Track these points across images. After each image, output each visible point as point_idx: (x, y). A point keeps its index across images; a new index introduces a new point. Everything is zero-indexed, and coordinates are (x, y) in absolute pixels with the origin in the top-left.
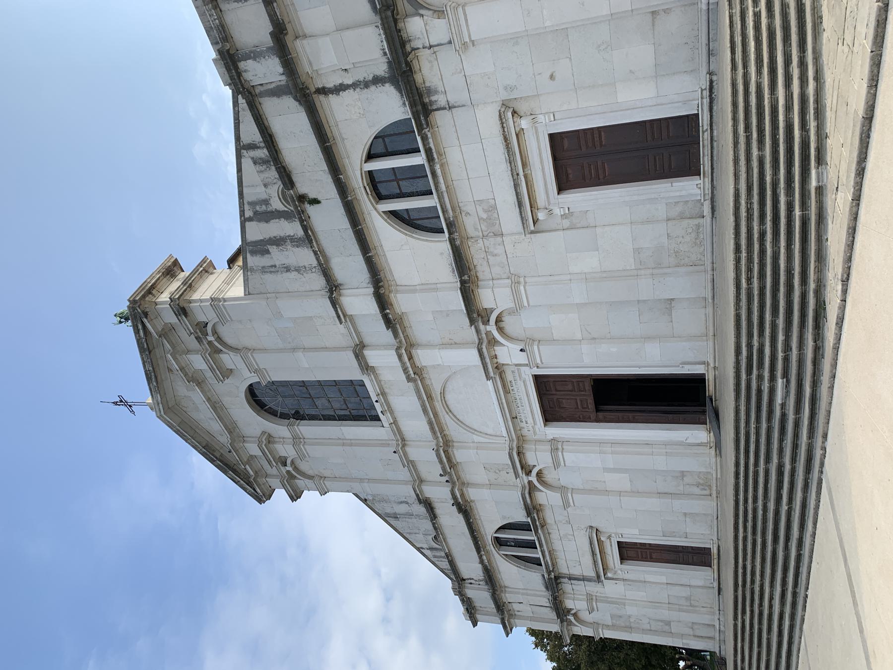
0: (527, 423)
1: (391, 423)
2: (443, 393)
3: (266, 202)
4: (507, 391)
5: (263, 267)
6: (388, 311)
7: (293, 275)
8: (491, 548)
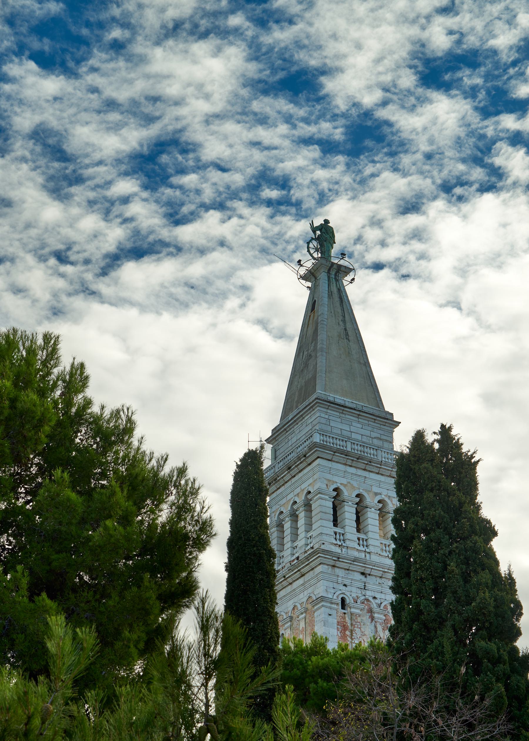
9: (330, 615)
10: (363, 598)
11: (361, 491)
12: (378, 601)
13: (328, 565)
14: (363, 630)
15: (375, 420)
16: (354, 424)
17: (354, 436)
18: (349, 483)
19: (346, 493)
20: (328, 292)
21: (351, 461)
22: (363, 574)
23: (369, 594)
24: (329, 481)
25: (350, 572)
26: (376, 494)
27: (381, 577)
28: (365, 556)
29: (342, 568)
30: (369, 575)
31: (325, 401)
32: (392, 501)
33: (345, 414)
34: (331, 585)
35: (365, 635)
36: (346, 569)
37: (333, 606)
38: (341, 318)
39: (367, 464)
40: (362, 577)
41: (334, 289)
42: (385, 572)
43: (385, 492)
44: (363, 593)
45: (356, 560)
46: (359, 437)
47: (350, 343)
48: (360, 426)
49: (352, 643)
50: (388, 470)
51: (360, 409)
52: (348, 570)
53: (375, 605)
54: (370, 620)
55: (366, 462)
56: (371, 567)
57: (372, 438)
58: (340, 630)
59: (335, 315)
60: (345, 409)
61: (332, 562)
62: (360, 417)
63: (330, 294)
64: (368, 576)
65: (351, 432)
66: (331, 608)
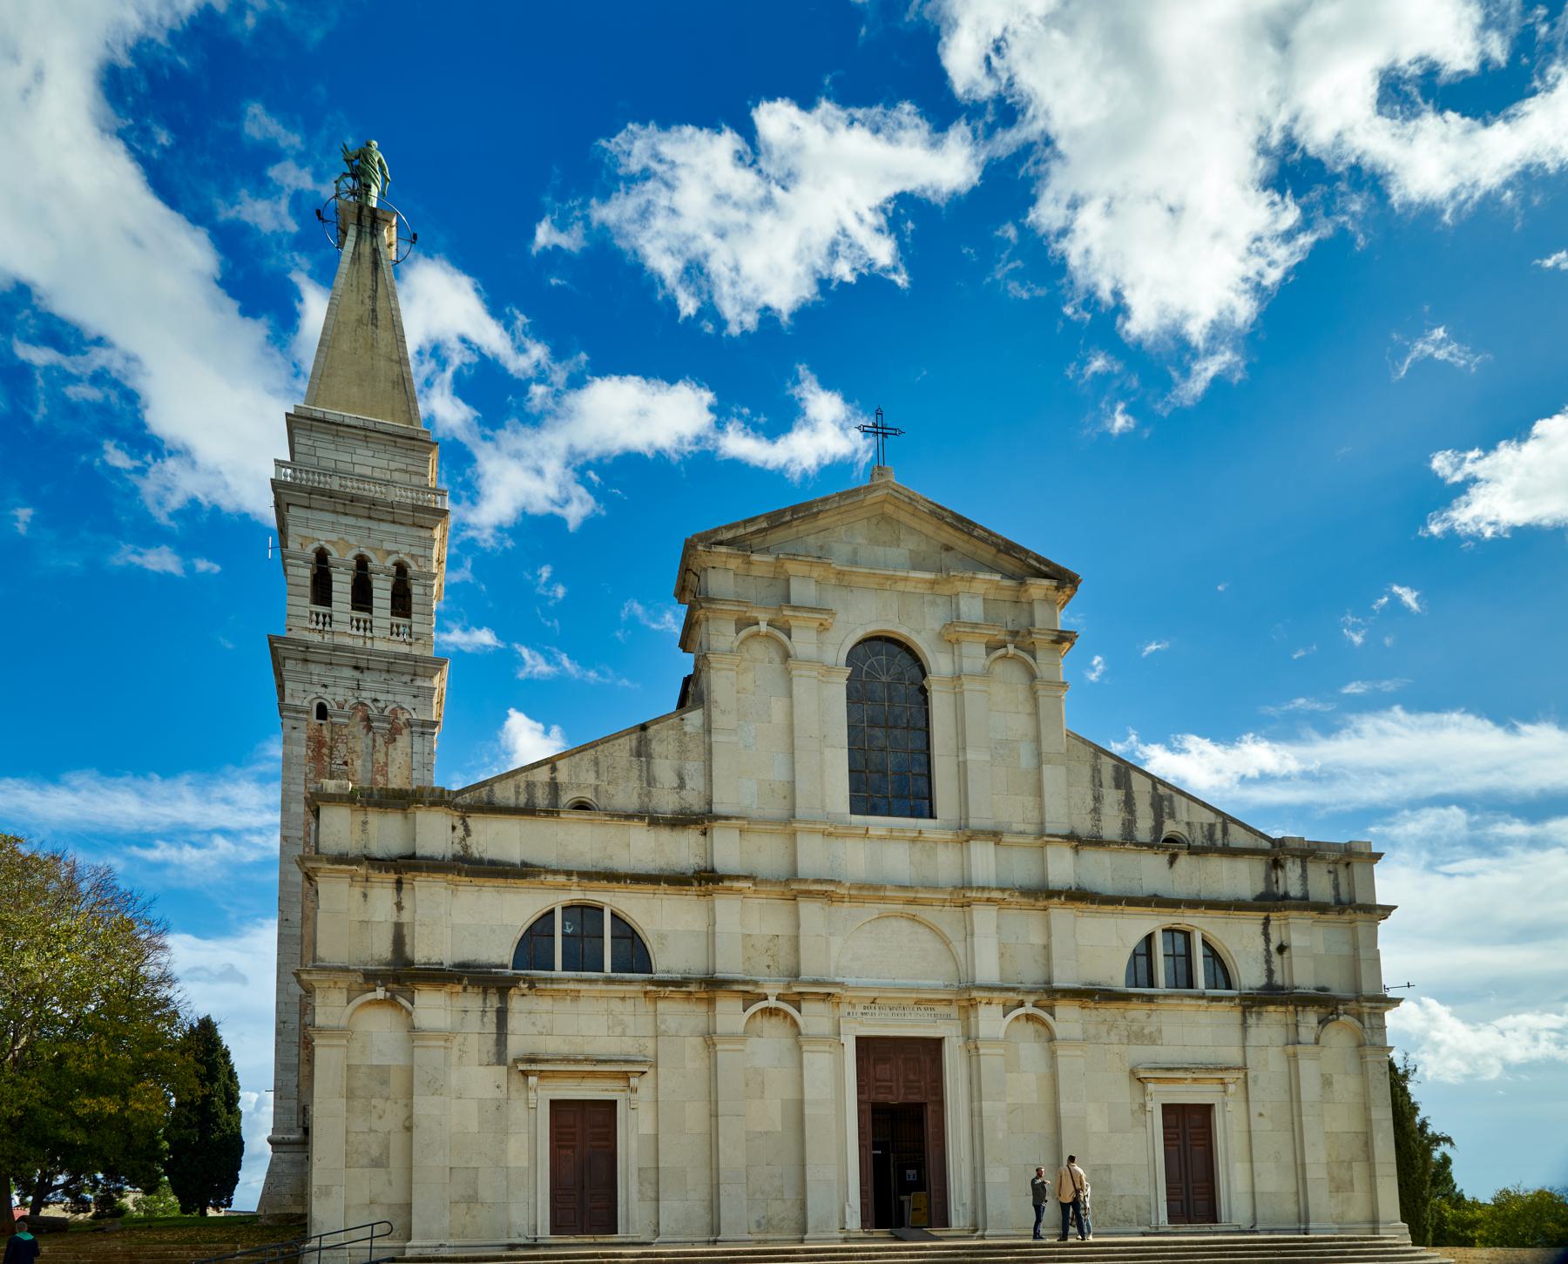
0: (862, 1014)
1: (867, 831)
2: (913, 918)
3: (1172, 815)
4: (918, 1002)
5: (1099, 771)
6: (1063, 899)
7: (1090, 803)
8: (576, 895)
9: (295, 728)
10: (355, 701)
12: (381, 705)
13: (296, 659)
14: (350, 745)
19: (375, 562)
22: (356, 668)
23: (366, 696)
28: (365, 643)
29: (321, 663)
30: (368, 669)
35: (355, 752)
36: (326, 664)
37: (301, 715)
40: (357, 674)
42: (392, 663)
43: (406, 549)
49: (331, 764)
52: (331, 664)
53: (376, 711)
61: (301, 656)
64: (365, 671)
66: (296, 719)
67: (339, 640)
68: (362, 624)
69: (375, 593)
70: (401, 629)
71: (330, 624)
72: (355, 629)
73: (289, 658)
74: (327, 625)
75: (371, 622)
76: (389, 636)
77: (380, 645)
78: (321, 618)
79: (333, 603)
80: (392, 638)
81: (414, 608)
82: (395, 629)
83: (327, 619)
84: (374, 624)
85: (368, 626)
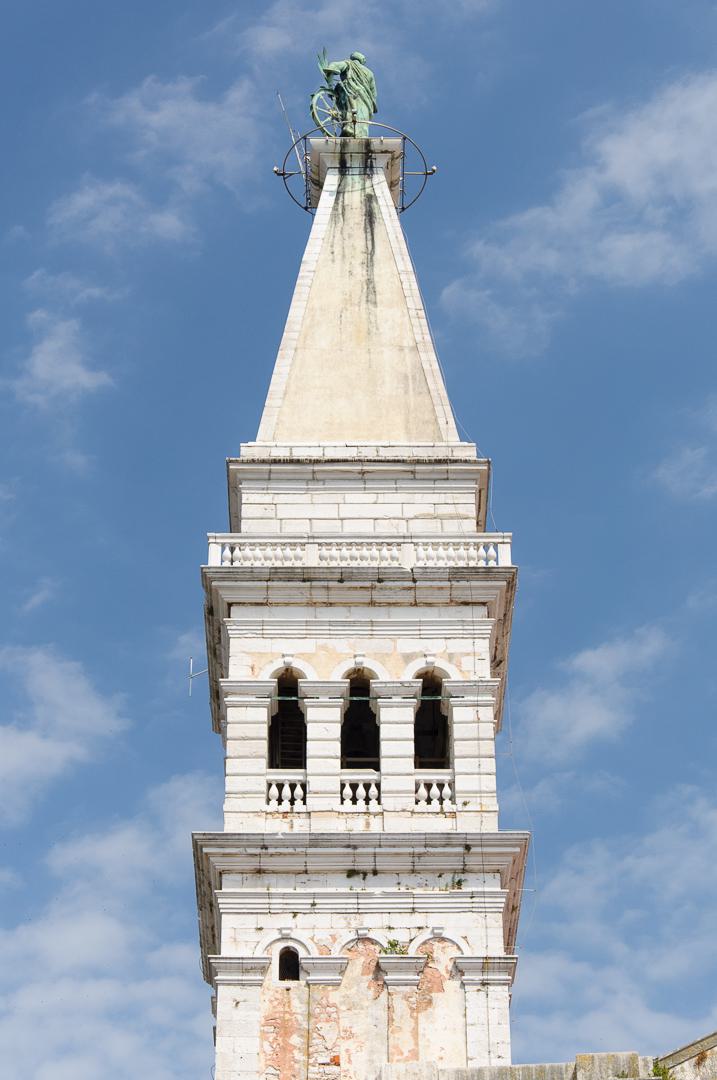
11: (359, 659)
15: (413, 472)
16: (351, 497)
17: (350, 528)
18: (324, 647)
20: (335, 209)
21: (324, 592)
24: (261, 655)
25: (314, 877)
26: (408, 658)
27: (413, 871)
28: (368, 824)
30: (375, 873)
31: (263, 462)
32: (459, 666)
33: (324, 481)
34: (251, 921)
38: (361, 257)
39: (373, 588)
41: (354, 199)
42: (420, 855)
44: (354, 924)
45: (317, 841)
46: (366, 528)
47: (379, 309)
48: (371, 497)
50: (441, 588)
51: (372, 455)
52: (306, 872)
54: (371, 993)
55: (368, 584)
56: (371, 850)
57: (408, 519)
58: (271, 1037)
59: (344, 256)
60: (317, 468)
61: (254, 863)
62: (366, 476)
63: (340, 211)
65: (342, 519)
67: (321, 825)
68: (361, 791)
69: (385, 731)
70: (435, 790)
71: (304, 800)
72: (348, 802)
73: (229, 872)
74: (299, 803)
75: (378, 786)
76: (412, 806)
77: (397, 825)
78: (287, 791)
79: (309, 761)
80: (417, 808)
81: (458, 748)
82: (423, 791)
83: (299, 791)
84: (382, 788)
85: (372, 793)
